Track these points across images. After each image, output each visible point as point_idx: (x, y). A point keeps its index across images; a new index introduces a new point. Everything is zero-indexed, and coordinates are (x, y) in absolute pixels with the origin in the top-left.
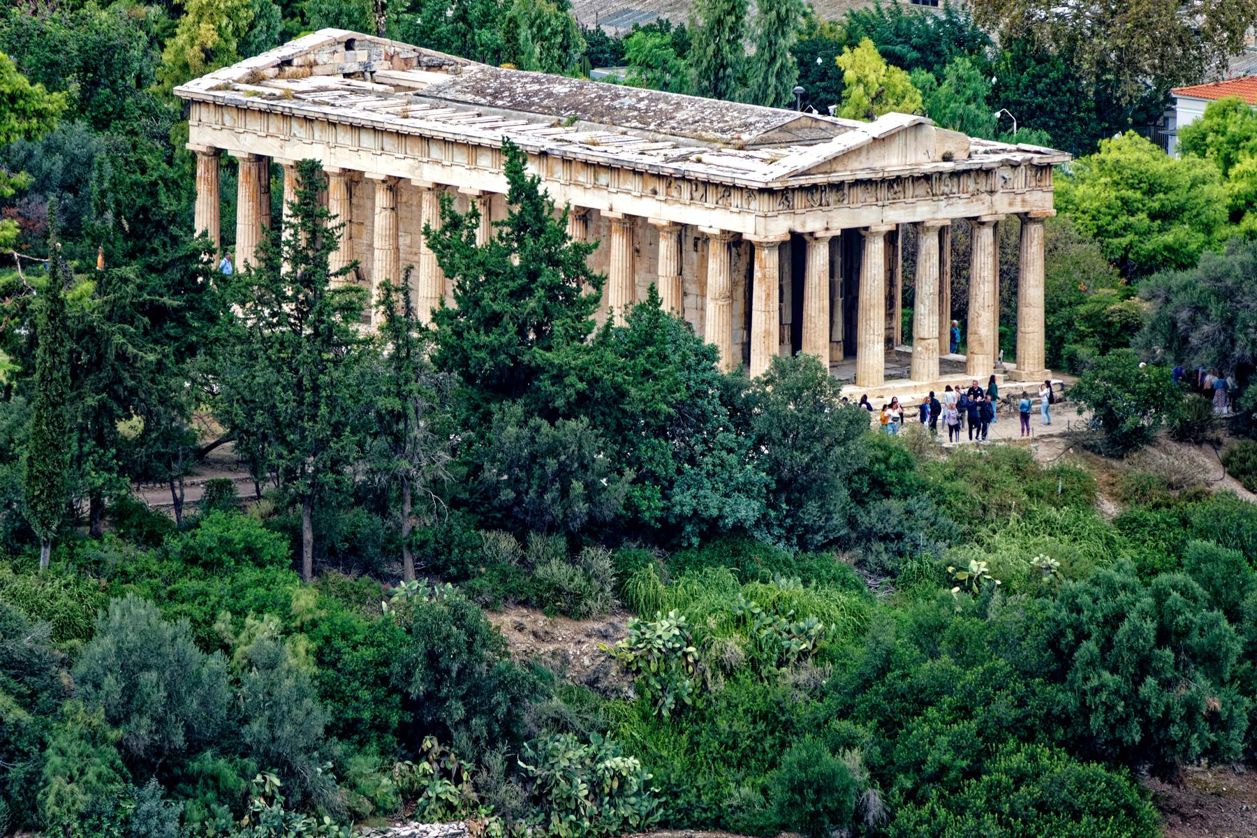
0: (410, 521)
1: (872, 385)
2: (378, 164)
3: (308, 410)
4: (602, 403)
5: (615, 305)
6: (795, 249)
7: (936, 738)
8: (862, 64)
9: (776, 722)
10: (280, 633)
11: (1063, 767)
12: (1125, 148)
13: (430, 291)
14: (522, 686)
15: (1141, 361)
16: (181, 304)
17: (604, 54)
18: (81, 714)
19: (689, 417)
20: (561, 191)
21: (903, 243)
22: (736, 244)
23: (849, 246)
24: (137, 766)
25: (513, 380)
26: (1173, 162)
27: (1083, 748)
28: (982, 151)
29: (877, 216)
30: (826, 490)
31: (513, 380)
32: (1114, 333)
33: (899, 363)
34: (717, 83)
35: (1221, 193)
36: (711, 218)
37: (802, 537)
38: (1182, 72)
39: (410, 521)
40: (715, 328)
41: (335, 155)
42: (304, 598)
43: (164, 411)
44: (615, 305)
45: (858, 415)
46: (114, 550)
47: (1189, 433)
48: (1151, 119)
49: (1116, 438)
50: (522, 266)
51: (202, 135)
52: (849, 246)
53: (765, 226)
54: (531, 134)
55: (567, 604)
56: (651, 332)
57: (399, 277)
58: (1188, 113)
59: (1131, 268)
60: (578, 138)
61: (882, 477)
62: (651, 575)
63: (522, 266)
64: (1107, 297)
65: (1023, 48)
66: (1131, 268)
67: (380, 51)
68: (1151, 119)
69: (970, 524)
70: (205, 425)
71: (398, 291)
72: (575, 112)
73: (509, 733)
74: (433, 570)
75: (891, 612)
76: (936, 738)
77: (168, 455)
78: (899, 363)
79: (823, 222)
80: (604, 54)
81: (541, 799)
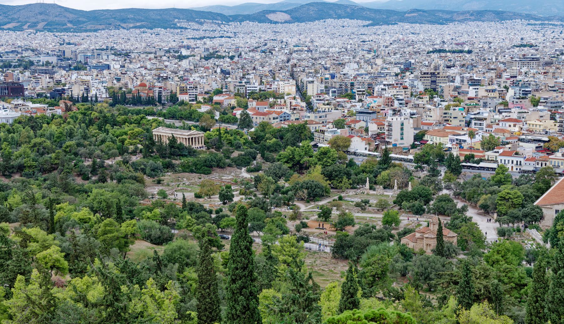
0: (167, 155)
1: (194, 146)
2: (164, 134)
3: (161, 149)
4: (178, 148)
5: (179, 142)
6: (189, 139)
7: (198, 167)
8: (192, 128)
9: (189, 166)
10: (160, 162)
11: (206, 168)
12: (208, 132)
13: (168, 142)
14: (174, 165)
15: (210, 144)
16: (153, 143)
17: (177, 128)
18: (148, 168)
19: (183, 149)
20: (175, 136)
21: (195, 138)
22: (186, 139)
23: (192, 138)
24: (152, 170)
25: (173, 147)
26: (211, 133)
27: (207, 167)
28: (200, 132)
29: (194, 136)
30: (191, 153)
31: (173, 147)
32: (208, 143)
33: (195, 145)
34: (184, 129)
35: (214, 134)
36: (184, 137)
37: (190, 155)
38: (211, 127)
39: (167, 155)
40: (184, 143)
41: (162, 134)
42: (161, 160)
43: (152, 149)
44: (179, 142)
45: (193, 148)
46: (150, 158)
47: (213, 148)
48: (209, 130)
49: (208, 149)
50: (173, 140)
51: (154, 133)
52: (192, 138)
53: (187, 137)
54: (173, 132)
55: (177, 160)
56: (181, 144)
57: (166, 141)
58: (212, 130)
59: (209, 139)
60: (176, 133)
61: (195, 152)
62: (181, 158)
63: (173, 140)
64: (207, 141)
65: (202, 126)
66: (209, 139)
67: (164, 128)
68: (209, 130)
69: (200, 154)
70: (155, 150)
71: (166, 142)
72: (176, 131)
73: (173, 167)
74: (169, 158)
75: (195, 159)
76: (198, 167)
77: (153, 152)
78: (195, 145)
79: (190, 137)
80: (177, 128)
81: (176, 171)
